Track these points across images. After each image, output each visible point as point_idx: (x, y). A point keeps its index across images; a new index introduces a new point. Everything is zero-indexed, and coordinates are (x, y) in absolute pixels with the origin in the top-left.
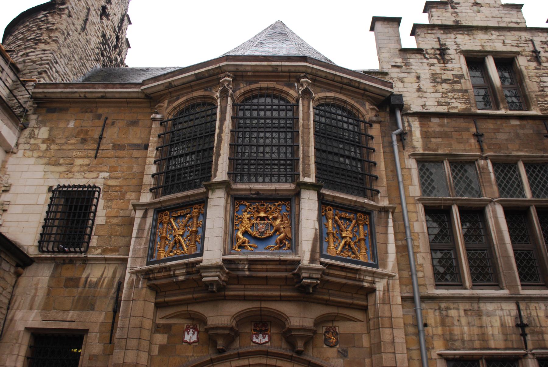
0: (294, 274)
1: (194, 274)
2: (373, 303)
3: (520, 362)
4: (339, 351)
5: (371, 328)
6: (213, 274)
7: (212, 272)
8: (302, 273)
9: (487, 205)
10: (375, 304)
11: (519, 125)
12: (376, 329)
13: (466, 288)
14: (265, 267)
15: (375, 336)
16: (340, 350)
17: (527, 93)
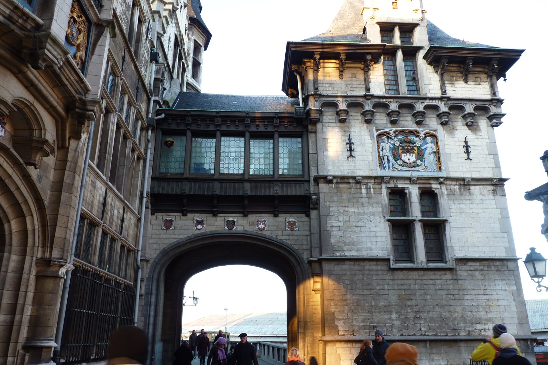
0: (81, 99)
1: (14, 24)
2: (74, 149)
3: (96, 228)
4: (38, 176)
5: (67, 168)
6: (55, 53)
7: (55, 50)
8: (95, 106)
9: (113, 112)
10: (75, 150)
11: (133, 71)
12: (71, 172)
13: (94, 163)
14: (70, 75)
15: (68, 176)
16: (39, 174)
17: (139, 52)
